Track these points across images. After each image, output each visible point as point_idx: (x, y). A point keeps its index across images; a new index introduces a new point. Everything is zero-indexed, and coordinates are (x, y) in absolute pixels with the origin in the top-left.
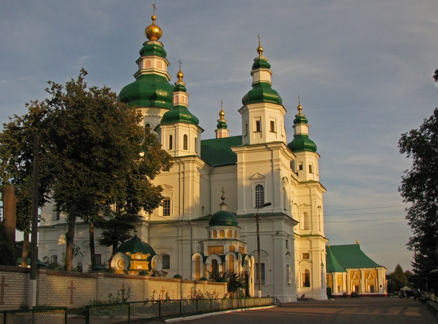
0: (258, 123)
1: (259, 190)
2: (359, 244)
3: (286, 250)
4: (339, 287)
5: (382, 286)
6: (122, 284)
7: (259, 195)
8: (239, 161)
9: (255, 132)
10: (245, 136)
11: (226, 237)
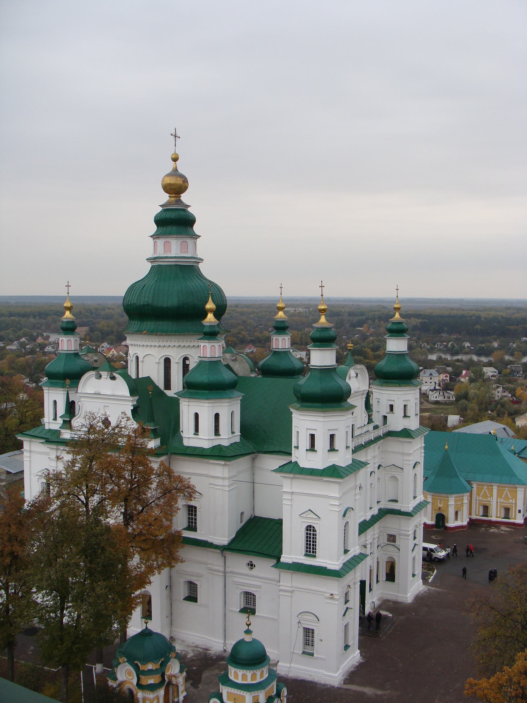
0: (312, 437)
1: (310, 530)
4: (456, 513)
7: (310, 538)
9: (307, 450)
10: (295, 447)
11: (249, 681)
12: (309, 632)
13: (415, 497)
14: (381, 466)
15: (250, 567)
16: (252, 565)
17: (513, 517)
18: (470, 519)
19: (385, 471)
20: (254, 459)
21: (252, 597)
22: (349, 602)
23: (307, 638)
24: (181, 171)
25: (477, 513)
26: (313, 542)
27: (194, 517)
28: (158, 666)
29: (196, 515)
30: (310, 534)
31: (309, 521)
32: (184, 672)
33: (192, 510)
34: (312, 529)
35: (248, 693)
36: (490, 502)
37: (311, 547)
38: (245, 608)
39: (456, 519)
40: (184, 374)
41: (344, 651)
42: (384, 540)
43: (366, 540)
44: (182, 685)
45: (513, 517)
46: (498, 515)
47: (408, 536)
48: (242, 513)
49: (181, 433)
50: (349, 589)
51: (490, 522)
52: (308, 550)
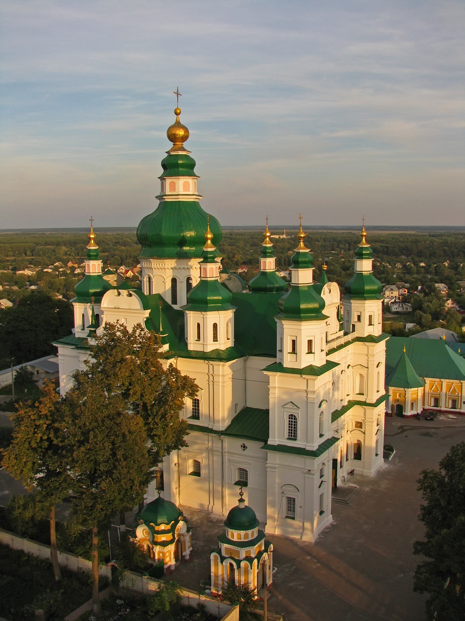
0: (294, 342)
4: (412, 404)
8: (271, 385)
9: (289, 353)
10: (279, 350)
12: (291, 501)
13: (378, 391)
14: (350, 367)
15: (243, 448)
16: (244, 447)
17: (459, 407)
18: (424, 409)
20: (245, 361)
21: (245, 472)
22: (324, 476)
23: (290, 505)
24: (182, 123)
25: (429, 404)
26: (294, 428)
27: (197, 408)
28: (169, 527)
29: (198, 406)
30: (292, 422)
31: (291, 411)
32: (190, 532)
33: (196, 403)
34: (293, 417)
35: (243, 549)
37: (293, 432)
38: (239, 481)
39: (412, 409)
40: (188, 291)
41: (319, 516)
43: (338, 427)
44: (188, 542)
45: (459, 407)
47: (372, 422)
48: (236, 405)
49: (186, 340)
50: (324, 466)
51: (440, 411)
52: (290, 434)
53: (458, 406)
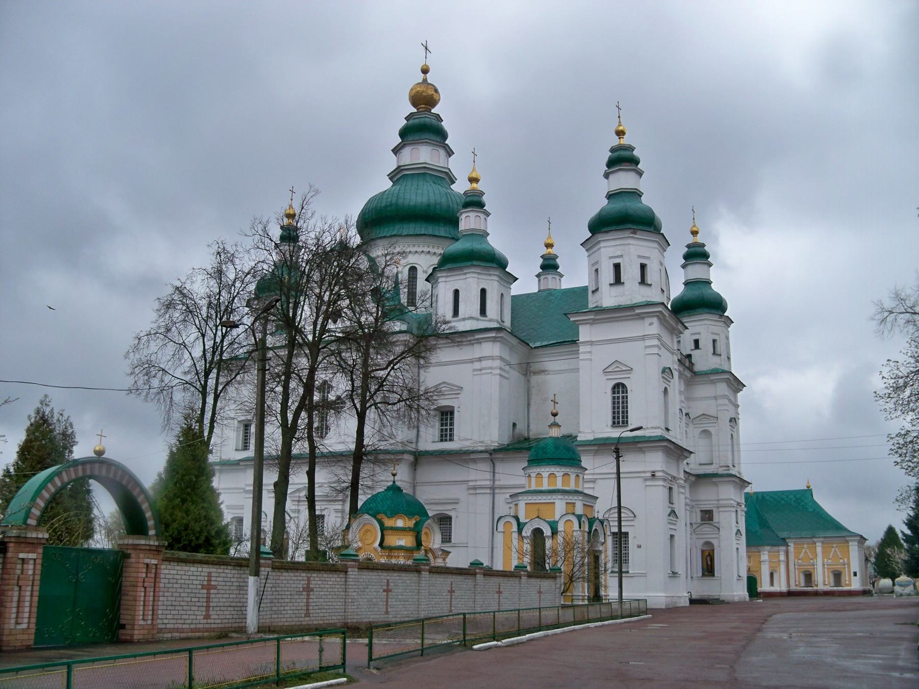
0: (617, 267)
2: (811, 489)
3: (669, 507)
4: (772, 575)
5: (858, 574)
6: (386, 581)
7: (618, 403)
9: (611, 285)
10: (593, 292)
11: (559, 485)
19: (694, 424)
25: (797, 583)
26: (623, 407)
29: (452, 424)
30: (618, 398)
36: (814, 565)
39: (772, 584)
42: (697, 518)
46: (827, 583)
51: (816, 594)
53: (846, 581)
